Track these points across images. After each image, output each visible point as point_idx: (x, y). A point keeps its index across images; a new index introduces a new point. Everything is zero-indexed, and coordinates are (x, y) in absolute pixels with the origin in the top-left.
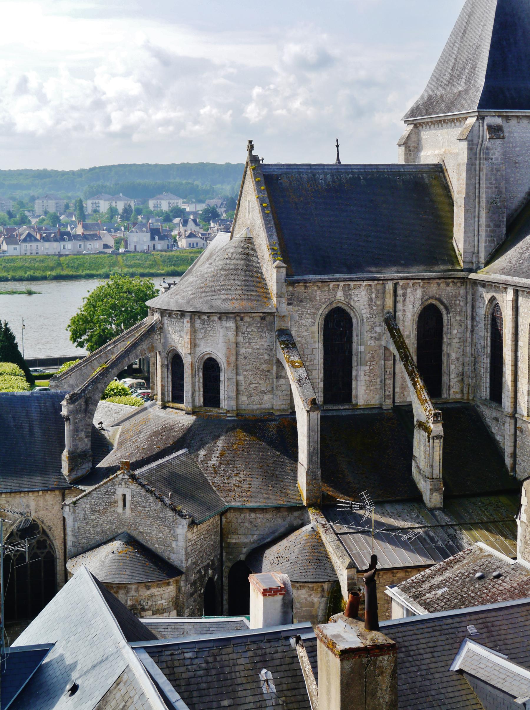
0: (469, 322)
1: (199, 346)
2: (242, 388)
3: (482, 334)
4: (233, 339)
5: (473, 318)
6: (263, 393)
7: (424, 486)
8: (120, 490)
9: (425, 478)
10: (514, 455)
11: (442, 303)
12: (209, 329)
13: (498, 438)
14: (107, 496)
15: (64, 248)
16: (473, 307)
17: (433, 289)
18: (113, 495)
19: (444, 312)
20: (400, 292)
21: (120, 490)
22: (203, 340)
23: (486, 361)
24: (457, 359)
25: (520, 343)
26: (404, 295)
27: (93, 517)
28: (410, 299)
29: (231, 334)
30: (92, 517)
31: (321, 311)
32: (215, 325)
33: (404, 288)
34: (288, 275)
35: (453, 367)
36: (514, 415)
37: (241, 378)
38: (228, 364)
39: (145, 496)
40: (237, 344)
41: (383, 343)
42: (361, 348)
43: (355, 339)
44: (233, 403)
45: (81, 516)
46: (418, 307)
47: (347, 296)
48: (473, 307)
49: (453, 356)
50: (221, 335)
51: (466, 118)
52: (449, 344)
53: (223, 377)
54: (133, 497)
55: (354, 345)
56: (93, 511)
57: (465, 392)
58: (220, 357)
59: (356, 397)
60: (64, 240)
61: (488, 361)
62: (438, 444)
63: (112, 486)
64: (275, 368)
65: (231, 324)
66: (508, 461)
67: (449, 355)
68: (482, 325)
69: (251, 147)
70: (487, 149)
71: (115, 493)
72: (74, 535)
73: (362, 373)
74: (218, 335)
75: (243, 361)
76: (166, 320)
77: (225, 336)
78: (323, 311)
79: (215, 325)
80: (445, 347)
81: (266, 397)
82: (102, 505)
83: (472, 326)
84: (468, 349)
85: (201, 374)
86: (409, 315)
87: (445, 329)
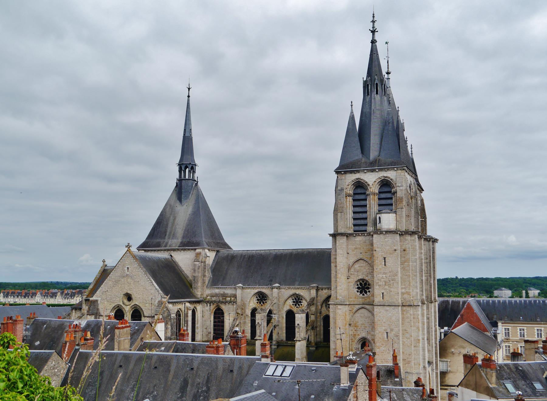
69: (104, 261)
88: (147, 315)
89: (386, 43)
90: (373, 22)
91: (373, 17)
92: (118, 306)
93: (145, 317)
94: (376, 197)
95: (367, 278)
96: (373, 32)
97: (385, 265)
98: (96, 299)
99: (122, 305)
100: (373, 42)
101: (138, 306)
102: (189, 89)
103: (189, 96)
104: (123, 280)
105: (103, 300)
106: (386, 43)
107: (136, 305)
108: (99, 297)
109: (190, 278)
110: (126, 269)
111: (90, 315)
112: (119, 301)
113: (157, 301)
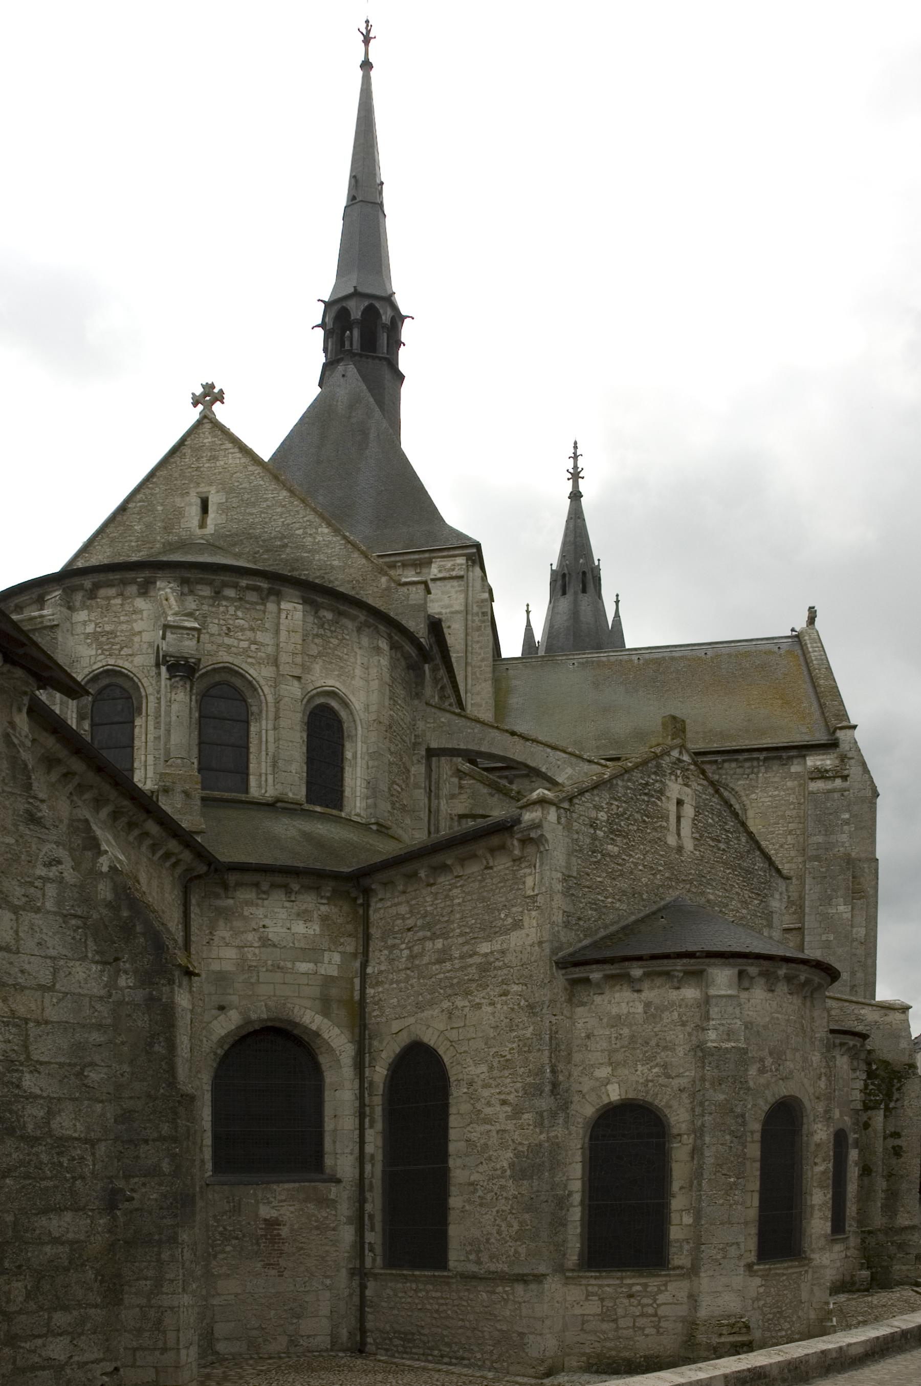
12: (335, 641)
14: (646, 798)
18: (659, 799)
22: (320, 661)
27: (613, 849)
30: (610, 847)
32: (348, 637)
39: (719, 815)
50: (359, 662)
54: (697, 813)
56: (612, 832)
63: (655, 773)
71: (661, 792)
74: (352, 660)
79: (348, 637)
82: (636, 820)
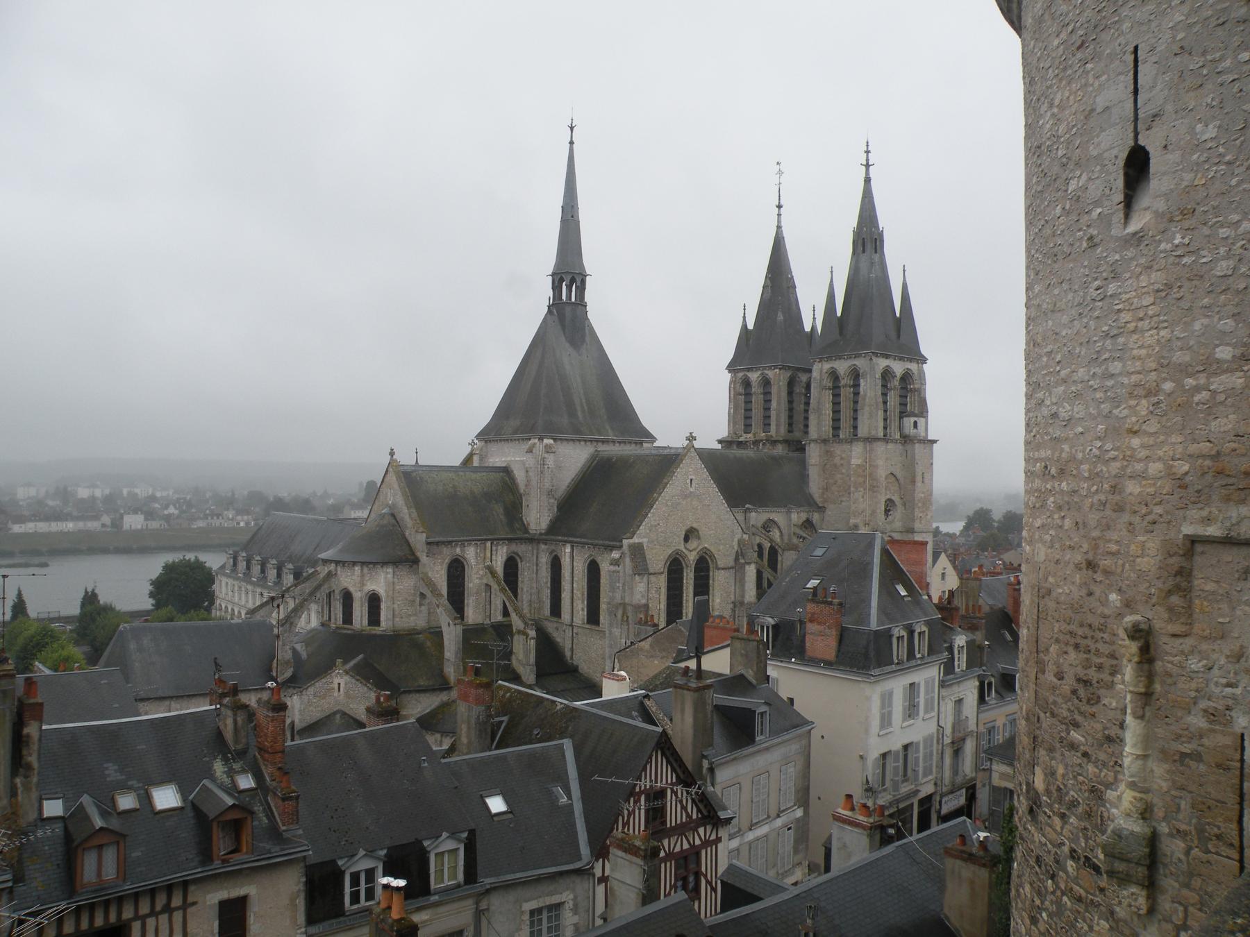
0: (535, 567)
1: (366, 585)
2: (396, 613)
3: (544, 575)
4: (391, 580)
5: (537, 565)
6: (410, 615)
7: (521, 670)
8: (336, 681)
9: (523, 665)
10: (572, 649)
11: (518, 555)
13: (558, 640)
15: (66, 527)
16: (537, 557)
17: (514, 547)
19: (519, 561)
20: (494, 548)
21: (336, 681)
23: (547, 593)
24: (527, 591)
25: (575, 579)
26: (497, 550)
28: (500, 552)
29: (390, 576)
31: (447, 561)
33: (497, 545)
34: (427, 538)
35: (524, 596)
36: (571, 625)
37: (396, 606)
38: (388, 596)
40: (394, 583)
41: (485, 581)
42: (471, 585)
43: (466, 579)
44: (390, 623)
45: (306, 701)
46: (505, 558)
47: (462, 551)
48: (537, 557)
49: (525, 590)
51: (530, 439)
52: (522, 582)
53: (383, 606)
54: (346, 684)
55: (466, 583)
57: (532, 612)
58: (381, 590)
59: (468, 617)
60: (67, 520)
61: (549, 591)
62: (533, 642)
64: (418, 599)
65: (390, 570)
66: (568, 654)
67: (522, 589)
68: (544, 568)
69: (392, 453)
70: (544, 458)
72: (300, 714)
73: (471, 601)
75: (397, 595)
76: (339, 568)
77: (386, 578)
78: (447, 561)
80: (520, 584)
81: (412, 618)
83: (537, 570)
84: (534, 585)
85: (367, 605)
86: (499, 563)
87: (519, 572)
88: (722, 566)
89: (778, 163)
90: (867, 152)
91: (867, 146)
92: (678, 552)
93: (719, 569)
94: (898, 392)
95: (893, 498)
96: (867, 166)
97: (923, 482)
98: (640, 541)
99: (684, 550)
100: (868, 180)
101: (709, 550)
102: (572, 128)
103: (571, 143)
104: (684, 503)
105: (653, 542)
106: (778, 163)
107: (706, 548)
108: (644, 537)
109: (522, 491)
110: (689, 481)
111: (639, 575)
112: (680, 543)
113: (736, 540)
